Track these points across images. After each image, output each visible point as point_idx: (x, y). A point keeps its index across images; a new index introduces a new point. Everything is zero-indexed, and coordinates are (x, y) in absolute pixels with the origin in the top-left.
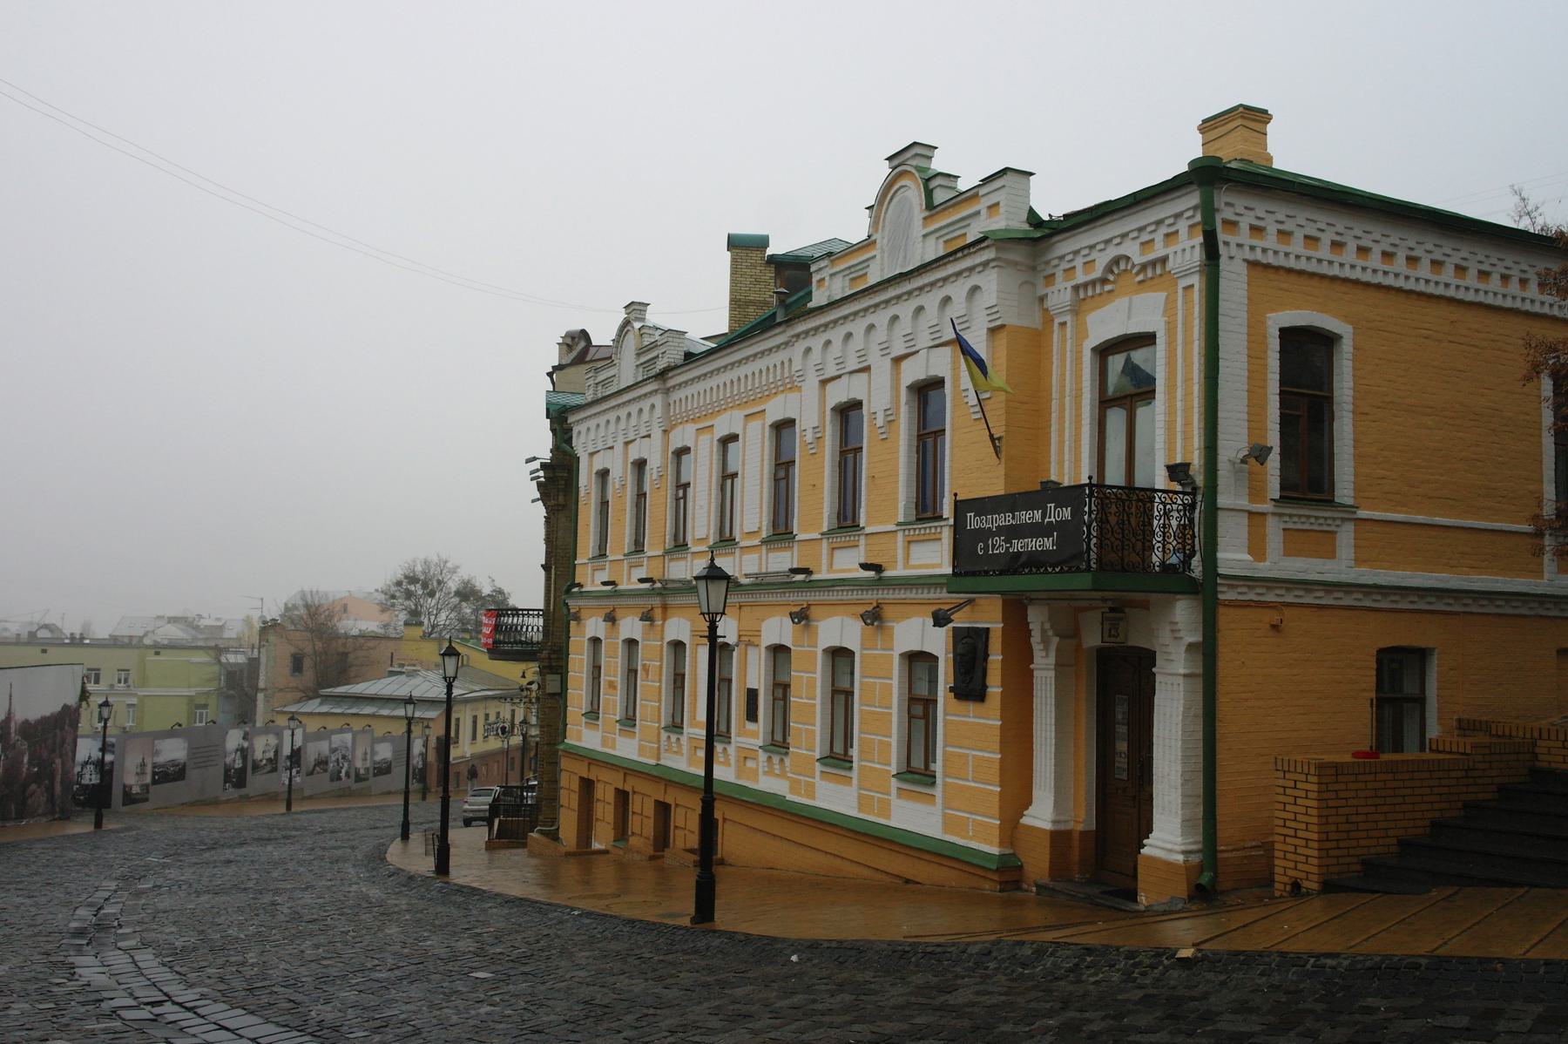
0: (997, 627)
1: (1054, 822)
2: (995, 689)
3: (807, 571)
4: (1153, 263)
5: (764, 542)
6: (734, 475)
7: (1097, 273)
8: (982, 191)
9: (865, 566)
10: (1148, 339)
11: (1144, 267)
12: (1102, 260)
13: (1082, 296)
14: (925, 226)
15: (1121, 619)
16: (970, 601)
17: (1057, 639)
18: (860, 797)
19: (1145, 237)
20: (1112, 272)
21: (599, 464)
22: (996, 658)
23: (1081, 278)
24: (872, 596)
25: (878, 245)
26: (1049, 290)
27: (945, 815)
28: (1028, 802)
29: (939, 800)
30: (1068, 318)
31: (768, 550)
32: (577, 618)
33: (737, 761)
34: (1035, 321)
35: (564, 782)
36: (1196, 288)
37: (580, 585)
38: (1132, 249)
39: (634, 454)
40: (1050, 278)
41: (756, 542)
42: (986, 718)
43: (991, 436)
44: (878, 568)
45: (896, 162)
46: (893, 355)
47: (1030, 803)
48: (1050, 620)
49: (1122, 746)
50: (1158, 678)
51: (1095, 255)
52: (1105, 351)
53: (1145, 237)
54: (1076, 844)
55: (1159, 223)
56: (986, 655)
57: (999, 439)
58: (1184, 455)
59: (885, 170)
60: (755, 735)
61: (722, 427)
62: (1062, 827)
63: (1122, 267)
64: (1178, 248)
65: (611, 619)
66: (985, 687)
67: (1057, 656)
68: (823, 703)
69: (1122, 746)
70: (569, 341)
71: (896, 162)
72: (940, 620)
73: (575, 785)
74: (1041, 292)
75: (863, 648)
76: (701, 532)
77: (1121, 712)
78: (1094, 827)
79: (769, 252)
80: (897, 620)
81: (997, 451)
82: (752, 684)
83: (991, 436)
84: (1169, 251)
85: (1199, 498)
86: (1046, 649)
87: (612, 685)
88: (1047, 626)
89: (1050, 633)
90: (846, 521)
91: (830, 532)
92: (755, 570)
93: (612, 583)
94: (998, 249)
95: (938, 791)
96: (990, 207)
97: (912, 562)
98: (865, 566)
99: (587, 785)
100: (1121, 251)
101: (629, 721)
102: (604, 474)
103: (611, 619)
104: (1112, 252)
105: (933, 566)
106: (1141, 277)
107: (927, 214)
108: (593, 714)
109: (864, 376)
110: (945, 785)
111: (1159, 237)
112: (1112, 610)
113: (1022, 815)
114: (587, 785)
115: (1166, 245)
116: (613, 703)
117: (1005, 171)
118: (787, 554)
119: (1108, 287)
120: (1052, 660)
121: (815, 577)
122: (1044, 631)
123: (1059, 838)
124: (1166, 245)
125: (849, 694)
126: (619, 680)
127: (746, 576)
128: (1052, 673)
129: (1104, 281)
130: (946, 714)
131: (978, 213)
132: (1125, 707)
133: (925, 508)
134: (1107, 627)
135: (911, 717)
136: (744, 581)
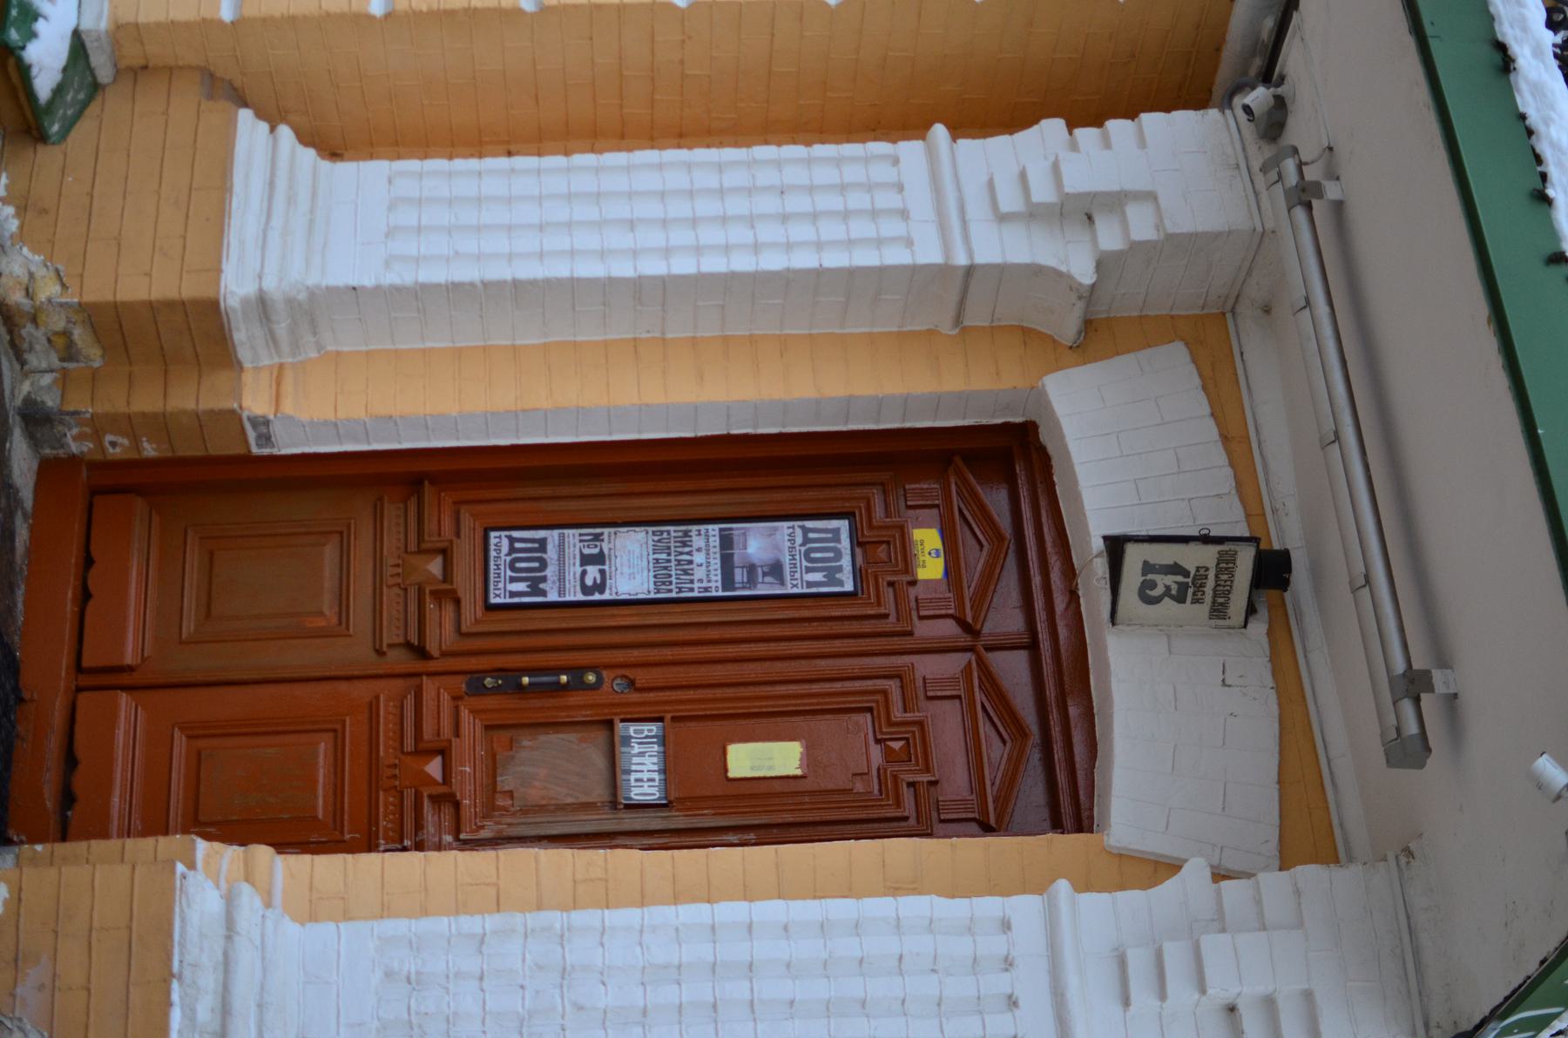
1: (262, 305)
15: (1219, 611)
17: (1083, 272)
47: (333, 154)
48: (1175, 245)
49: (632, 564)
50: (1025, 908)
54: (189, 397)
62: (242, 335)
67: (1001, 272)
69: (632, 564)
86: (1033, 214)
88: (1142, 225)
89: (1109, 238)
113: (272, 117)
120: (993, 246)
122: (1116, 202)
123: (195, 332)
128: (929, 253)
134: (1195, 557)
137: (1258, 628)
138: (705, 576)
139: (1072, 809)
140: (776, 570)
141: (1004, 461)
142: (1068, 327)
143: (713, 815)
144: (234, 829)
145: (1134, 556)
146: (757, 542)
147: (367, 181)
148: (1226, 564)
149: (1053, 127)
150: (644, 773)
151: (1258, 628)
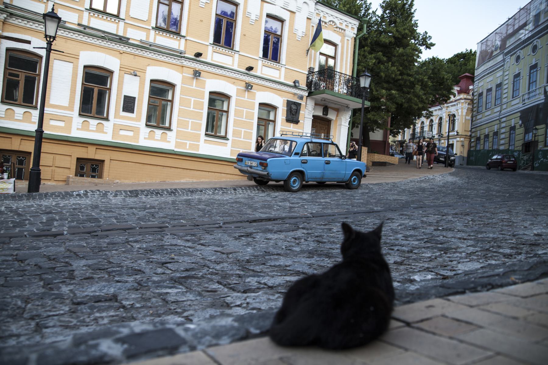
4: (340, 28)
5: (153, 28)
18: (231, 150)
19: (341, 21)
24: (248, 79)
31: (156, 34)
38: (337, 22)
51: (326, 15)
55: (346, 21)
60: (138, 119)
82: (132, 92)
92: (144, 39)
100: (335, 20)
104: (331, 18)
106: (336, 29)
111: (345, 23)
118: (177, 42)
136: (130, 41)
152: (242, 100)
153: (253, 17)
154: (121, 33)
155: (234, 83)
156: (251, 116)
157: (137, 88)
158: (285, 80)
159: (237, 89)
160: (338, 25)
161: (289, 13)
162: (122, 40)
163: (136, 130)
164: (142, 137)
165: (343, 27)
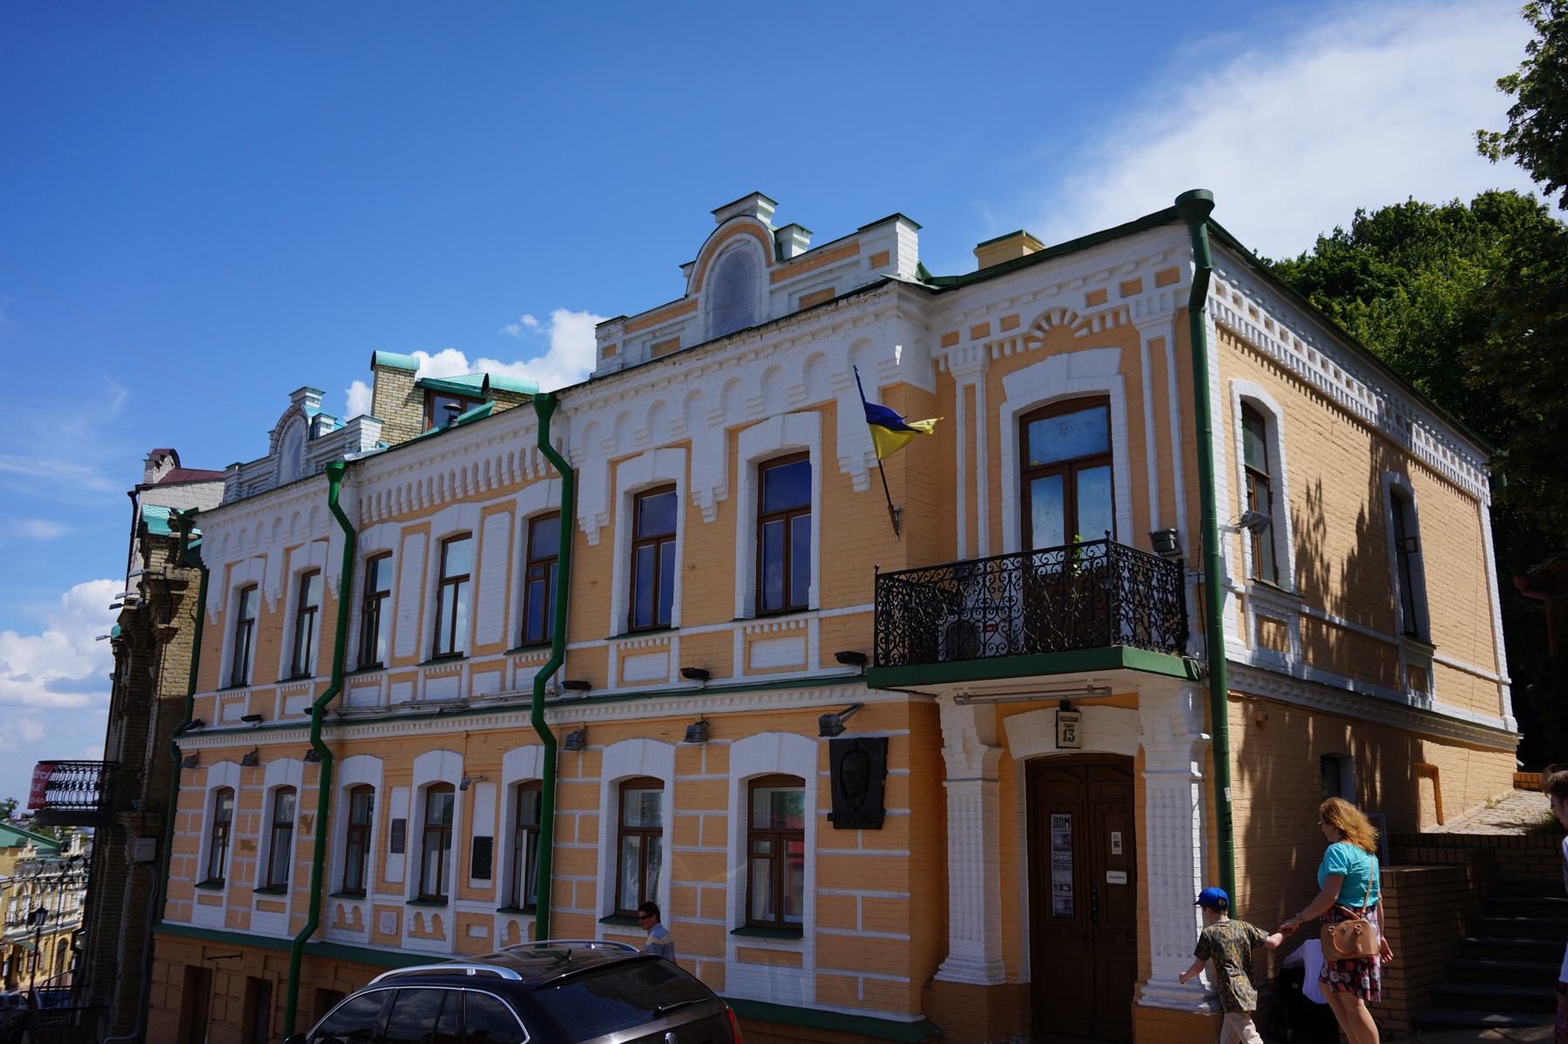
0: (900, 733)
2: (899, 808)
3: (584, 686)
5: (509, 653)
6: (458, 580)
7: (1024, 328)
8: (862, 239)
9: (688, 673)
10: (1101, 401)
11: (1088, 323)
12: (1028, 315)
13: (996, 354)
14: (772, 282)
15: (1076, 720)
16: (857, 707)
17: (985, 748)
20: (1039, 328)
21: (239, 577)
22: (899, 771)
23: (996, 334)
25: (701, 305)
26: (950, 350)
27: (818, 977)
28: (941, 951)
29: (809, 959)
30: (978, 382)
32: (195, 761)
33: (456, 930)
34: (931, 389)
35: (158, 971)
36: (1169, 339)
37: (199, 723)
38: (1074, 301)
39: (299, 562)
40: (950, 339)
41: (501, 656)
42: (887, 849)
43: (891, 507)
44: (703, 675)
45: (726, 215)
46: (727, 425)
49: (1062, 877)
52: (1025, 420)
53: (1093, 287)
55: (1111, 271)
56: (885, 772)
57: (899, 512)
58: (1161, 521)
59: (712, 223)
61: (444, 523)
63: (1055, 320)
64: (1142, 297)
65: (252, 760)
66: (883, 811)
68: (609, 847)
69: (1062, 877)
70: (157, 457)
71: (726, 215)
72: (828, 725)
73: (178, 976)
74: (937, 351)
75: (677, 771)
76: (406, 648)
77: (1060, 831)
78: (1024, 976)
79: (418, 376)
80: (738, 737)
81: (897, 526)
82: (482, 829)
83: (891, 507)
84: (1131, 300)
85: (1186, 571)
87: (247, 846)
88: (972, 733)
89: (976, 740)
90: (647, 618)
91: (620, 636)
93: (258, 718)
94: (900, 296)
95: (806, 947)
96: (872, 258)
97: (755, 664)
98: (688, 673)
99: (198, 979)
101: (274, 887)
102: (245, 592)
103: (252, 760)
105: (792, 669)
106: (1084, 332)
107: (777, 267)
108: (213, 882)
109: (682, 451)
110: (818, 937)
112: (1066, 705)
114: (198, 979)
115: (1123, 295)
116: (245, 866)
117: (897, 217)
119: (1032, 345)
121: (593, 693)
122: (965, 741)
123: (997, 994)
124: (1123, 295)
125: (651, 834)
126: (261, 837)
127: (482, 698)
129: (1028, 339)
130: (818, 844)
131: (857, 262)
132: (1068, 829)
133: (778, 596)
134: (1062, 728)
135: (752, 854)
137: (1081, 708)
138: (1066, 856)
139: (1129, 761)
140: (1065, 836)
141: (1036, 768)
142: (999, 752)
143: (1130, 862)
144: (1132, 992)
145: (1061, 743)
146: (1057, 840)
147: (956, 945)
148: (1063, 719)
149: (943, 751)
150: (1116, 877)
151: (1081, 708)
152: (693, 783)
153: (706, 502)
154: (464, 696)
155: (664, 737)
156: (717, 830)
157: (488, 814)
158: (822, 664)
159: (677, 750)
160: (1083, 311)
161: (816, 415)
162: (461, 709)
163: (487, 921)
164: (496, 943)
165: (1114, 300)
